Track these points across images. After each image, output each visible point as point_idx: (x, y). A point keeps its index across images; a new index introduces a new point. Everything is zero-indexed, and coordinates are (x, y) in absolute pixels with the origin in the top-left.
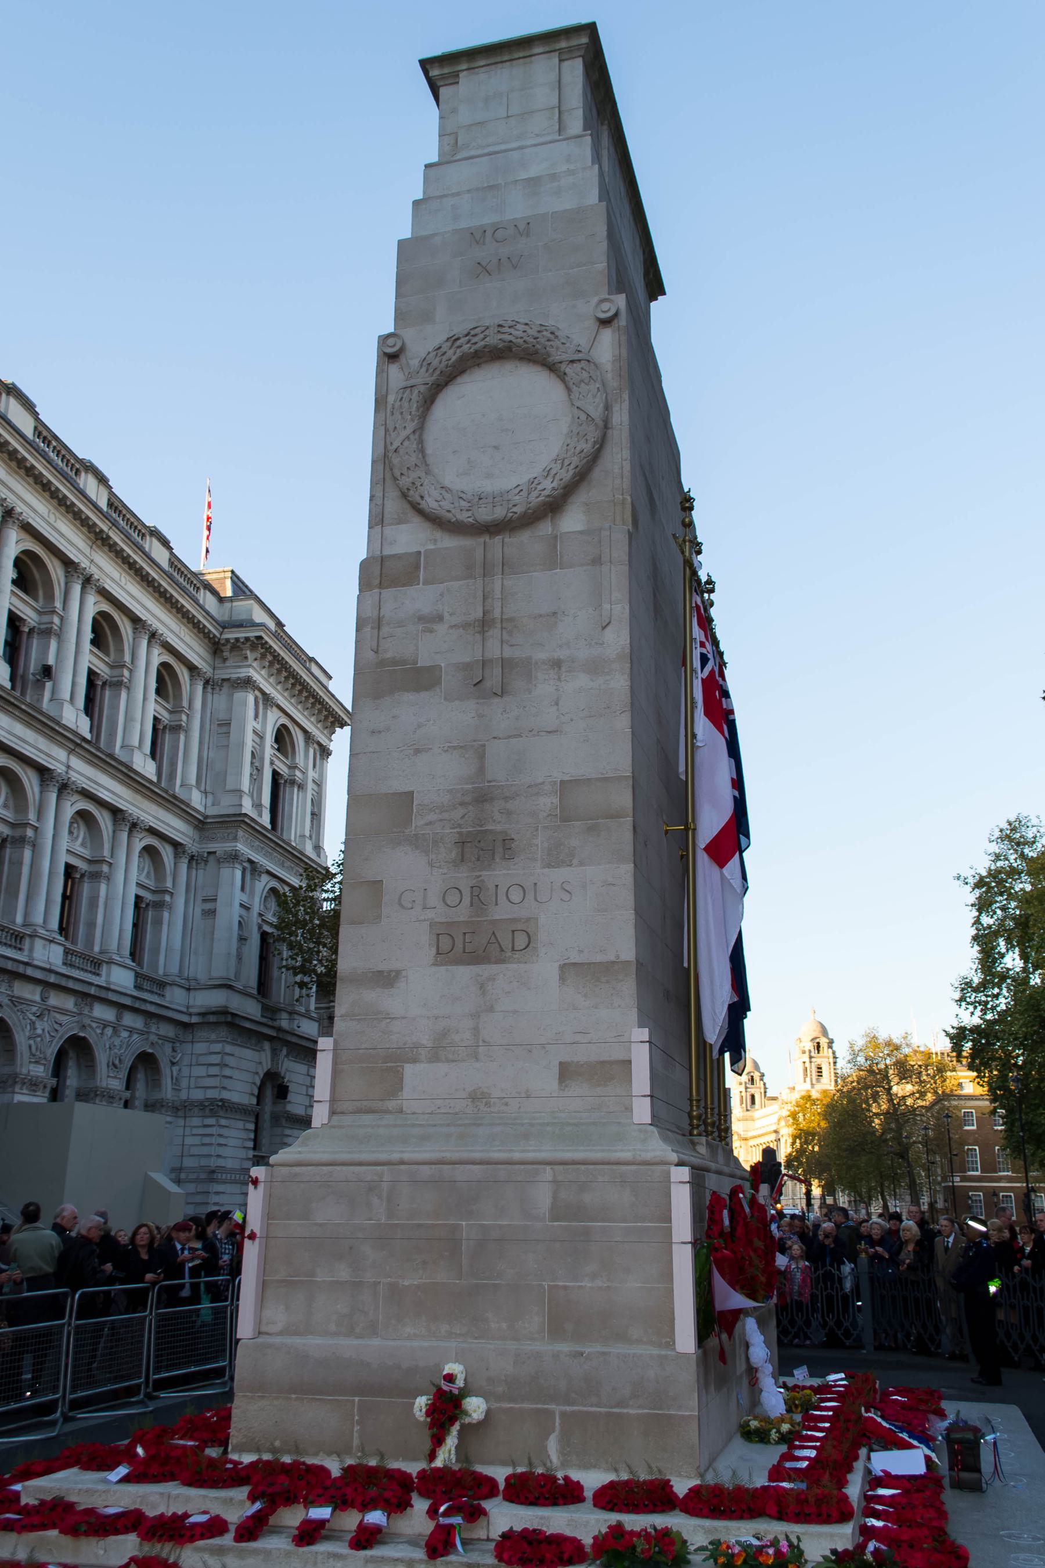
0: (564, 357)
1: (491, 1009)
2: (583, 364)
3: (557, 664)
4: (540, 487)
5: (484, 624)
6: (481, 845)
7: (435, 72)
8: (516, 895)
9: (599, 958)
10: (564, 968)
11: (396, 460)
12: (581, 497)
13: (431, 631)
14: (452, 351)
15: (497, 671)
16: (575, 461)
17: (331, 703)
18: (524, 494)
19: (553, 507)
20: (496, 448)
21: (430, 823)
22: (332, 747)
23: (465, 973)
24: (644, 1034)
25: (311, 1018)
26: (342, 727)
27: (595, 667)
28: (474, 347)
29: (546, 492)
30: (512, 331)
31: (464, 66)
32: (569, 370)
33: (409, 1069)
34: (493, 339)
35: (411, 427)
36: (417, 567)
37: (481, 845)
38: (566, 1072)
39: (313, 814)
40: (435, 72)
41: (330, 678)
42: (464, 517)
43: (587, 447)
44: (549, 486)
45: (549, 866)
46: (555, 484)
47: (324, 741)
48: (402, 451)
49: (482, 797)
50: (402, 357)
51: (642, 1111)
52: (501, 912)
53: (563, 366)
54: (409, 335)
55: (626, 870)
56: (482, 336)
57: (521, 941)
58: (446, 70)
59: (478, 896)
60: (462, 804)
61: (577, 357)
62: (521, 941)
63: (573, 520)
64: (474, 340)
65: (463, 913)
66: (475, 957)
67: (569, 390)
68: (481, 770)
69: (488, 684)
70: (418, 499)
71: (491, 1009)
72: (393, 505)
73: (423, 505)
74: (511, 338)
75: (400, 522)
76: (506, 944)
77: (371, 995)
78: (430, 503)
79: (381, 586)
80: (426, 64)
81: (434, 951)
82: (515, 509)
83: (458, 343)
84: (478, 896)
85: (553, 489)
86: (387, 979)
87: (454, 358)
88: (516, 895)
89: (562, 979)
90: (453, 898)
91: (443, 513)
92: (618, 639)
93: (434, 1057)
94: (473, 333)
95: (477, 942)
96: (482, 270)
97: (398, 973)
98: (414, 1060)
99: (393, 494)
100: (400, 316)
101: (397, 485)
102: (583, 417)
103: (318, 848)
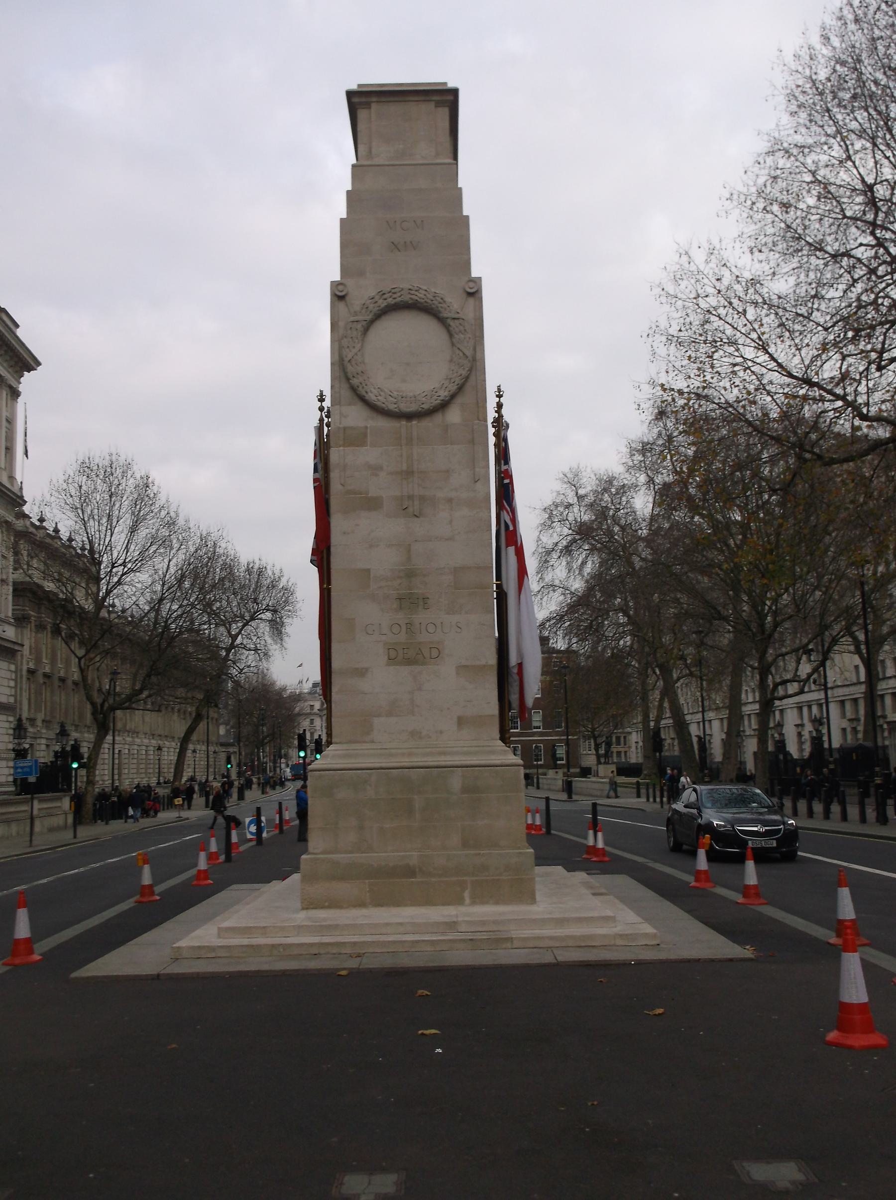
0: (449, 315)
1: (420, 689)
2: (461, 321)
3: (450, 500)
4: (437, 394)
5: (408, 474)
6: (410, 601)
7: (355, 100)
8: (431, 629)
9: (477, 663)
11: (350, 369)
12: (459, 400)
13: (377, 475)
14: (381, 301)
15: (417, 503)
16: (458, 381)
17: (21, 351)
18: (429, 397)
19: (444, 406)
20: (408, 364)
21: (380, 587)
22: (21, 388)
23: (405, 670)
25: (9, 623)
26: (30, 369)
28: (394, 301)
29: (441, 398)
30: (416, 293)
31: (374, 99)
32: (452, 323)
33: (376, 720)
34: (406, 298)
35: (358, 346)
36: (365, 435)
37: (410, 601)
39: (7, 448)
40: (355, 100)
41: (17, 326)
42: (392, 407)
43: (464, 373)
44: (444, 394)
45: (448, 614)
46: (446, 393)
47: (13, 383)
48: (353, 362)
49: (410, 574)
50: (347, 298)
53: (449, 321)
54: (350, 283)
56: (399, 294)
57: (435, 653)
58: (363, 100)
60: (399, 577)
61: (457, 316)
62: (435, 653)
63: (454, 415)
64: (395, 296)
65: (402, 637)
66: (409, 662)
67: (451, 335)
68: (409, 559)
69: (411, 509)
70: (364, 393)
71: (420, 689)
72: (346, 393)
73: (367, 397)
74: (416, 298)
75: (350, 404)
76: (427, 655)
78: (371, 397)
79: (344, 446)
80: (350, 94)
81: (386, 657)
82: (423, 406)
83: (385, 296)
85: (446, 396)
86: (361, 673)
87: (383, 306)
88: (431, 629)
89: (457, 674)
90: (396, 629)
91: (379, 403)
93: (390, 714)
94: (393, 291)
95: (410, 654)
96: (395, 246)
97: (367, 669)
98: (379, 716)
99: (345, 386)
100: (345, 269)
101: (350, 384)
102: (461, 354)
103: (12, 478)
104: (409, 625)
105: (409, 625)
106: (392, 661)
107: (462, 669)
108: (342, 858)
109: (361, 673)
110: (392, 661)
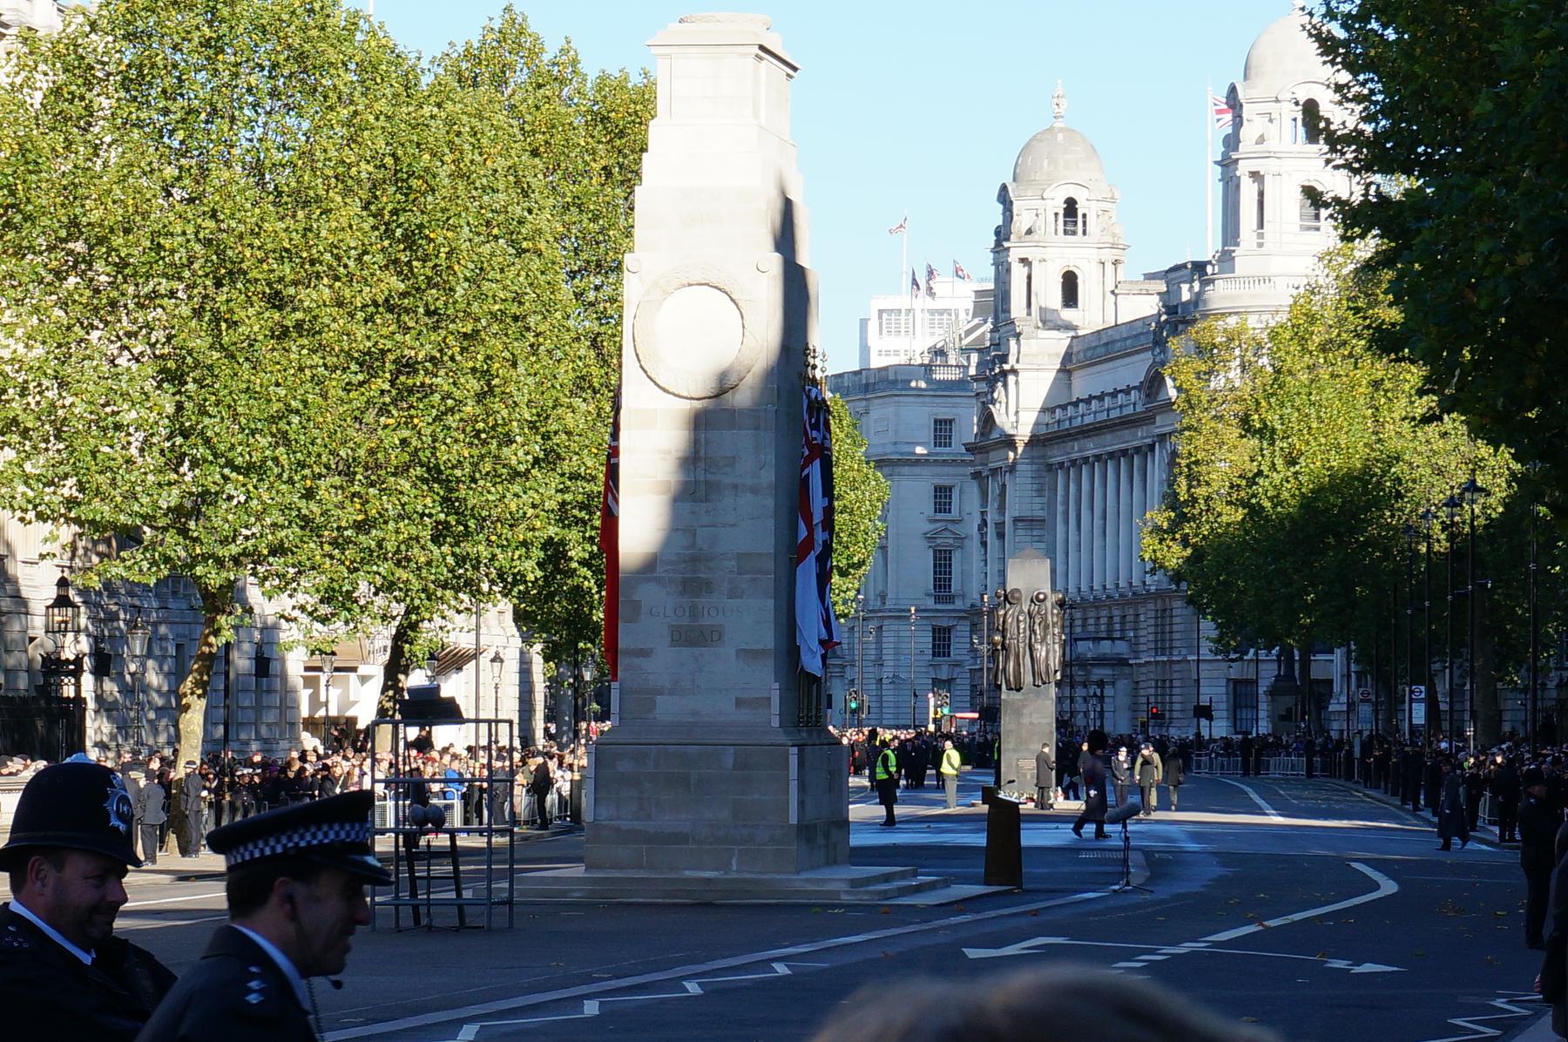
3: (735, 487)
8: (713, 613)
9: (755, 647)
10: (740, 652)
15: (703, 488)
24: (777, 686)
27: (755, 490)
38: (739, 703)
51: (775, 722)
52: (705, 621)
55: (771, 602)
59: (694, 613)
65: (685, 621)
66: (692, 643)
68: (693, 545)
77: (637, 661)
84: (694, 613)
86: (644, 653)
89: (737, 655)
90: (680, 613)
92: (768, 476)
95: (694, 636)
104: (693, 608)
105: (693, 608)
106: (675, 642)
107: (740, 652)
108: (624, 824)
109: (644, 653)
110: (675, 642)
